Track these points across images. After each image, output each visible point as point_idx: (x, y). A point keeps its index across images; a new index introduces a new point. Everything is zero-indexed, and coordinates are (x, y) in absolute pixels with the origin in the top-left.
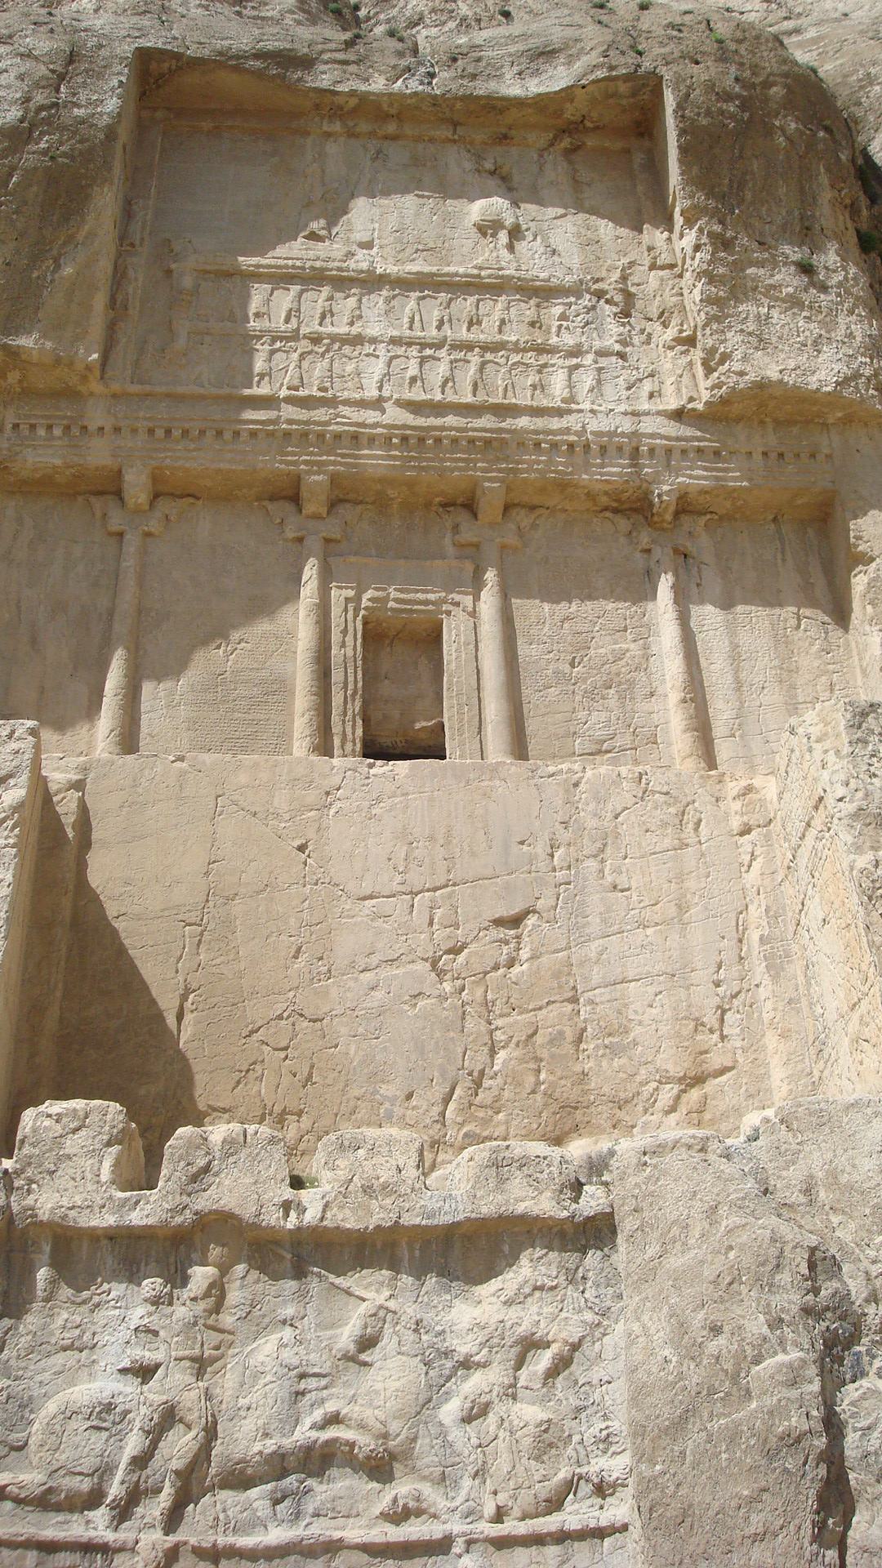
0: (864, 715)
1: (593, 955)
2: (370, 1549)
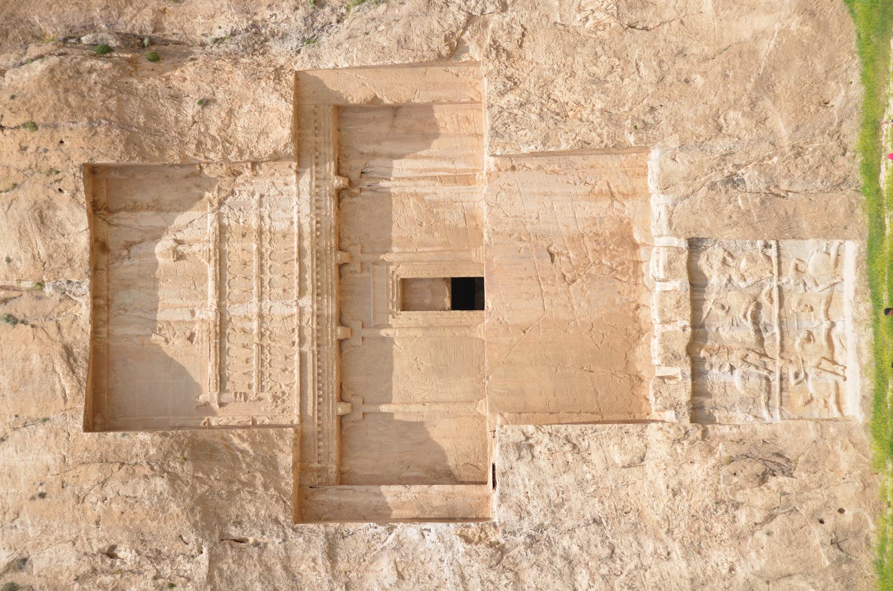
0: (497, 132)
1: (565, 228)
2: (781, 306)
